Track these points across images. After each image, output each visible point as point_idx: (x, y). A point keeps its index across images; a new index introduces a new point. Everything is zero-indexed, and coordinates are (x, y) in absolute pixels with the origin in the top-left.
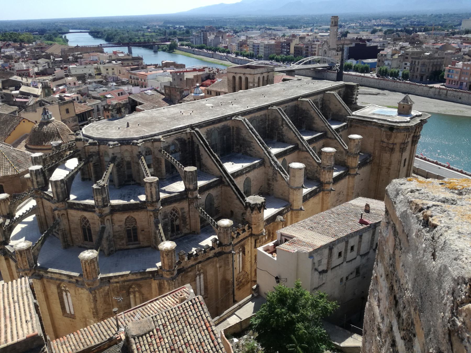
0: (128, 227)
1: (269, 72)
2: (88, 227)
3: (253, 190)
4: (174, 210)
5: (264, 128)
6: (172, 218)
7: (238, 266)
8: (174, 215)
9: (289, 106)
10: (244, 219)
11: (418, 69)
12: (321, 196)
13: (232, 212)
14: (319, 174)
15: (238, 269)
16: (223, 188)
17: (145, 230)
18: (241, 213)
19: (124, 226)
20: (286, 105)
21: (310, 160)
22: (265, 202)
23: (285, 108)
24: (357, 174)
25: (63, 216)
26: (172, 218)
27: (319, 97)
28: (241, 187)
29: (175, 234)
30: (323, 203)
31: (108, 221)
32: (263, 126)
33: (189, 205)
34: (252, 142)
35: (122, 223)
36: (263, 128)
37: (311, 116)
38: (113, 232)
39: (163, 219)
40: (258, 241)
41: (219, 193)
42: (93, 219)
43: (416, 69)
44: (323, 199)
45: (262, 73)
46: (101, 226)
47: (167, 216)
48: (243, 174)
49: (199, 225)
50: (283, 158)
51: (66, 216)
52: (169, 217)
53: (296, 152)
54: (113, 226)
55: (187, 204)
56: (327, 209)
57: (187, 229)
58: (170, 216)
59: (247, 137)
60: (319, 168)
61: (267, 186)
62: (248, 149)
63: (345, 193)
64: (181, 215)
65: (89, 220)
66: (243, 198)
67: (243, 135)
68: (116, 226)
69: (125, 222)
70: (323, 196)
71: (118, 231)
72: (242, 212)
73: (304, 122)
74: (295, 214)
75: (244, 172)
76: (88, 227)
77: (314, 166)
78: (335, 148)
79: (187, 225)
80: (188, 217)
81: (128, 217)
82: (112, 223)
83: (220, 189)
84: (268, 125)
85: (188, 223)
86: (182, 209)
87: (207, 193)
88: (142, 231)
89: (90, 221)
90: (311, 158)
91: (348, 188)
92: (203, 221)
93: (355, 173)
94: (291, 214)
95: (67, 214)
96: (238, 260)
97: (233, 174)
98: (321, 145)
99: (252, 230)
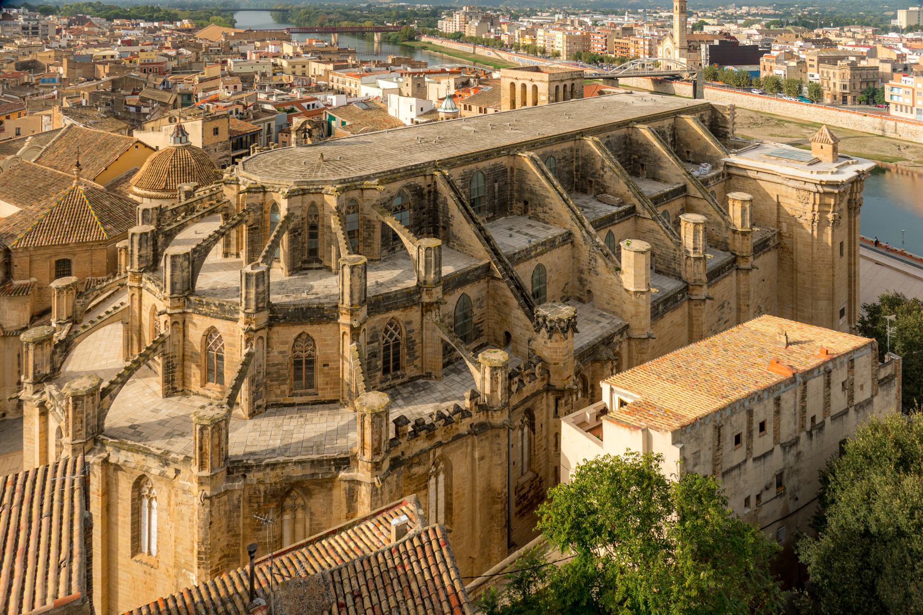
0: (298, 357)
1: (573, 79)
2: (220, 350)
3: (549, 293)
4: (391, 324)
5: (570, 173)
6: (387, 342)
7: (520, 458)
8: (391, 335)
9: (613, 135)
10: (533, 350)
11: (834, 84)
12: (686, 310)
13: (508, 336)
14: (680, 265)
15: (520, 464)
16: (491, 284)
17: (331, 364)
18: (527, 338)
19: (290, 353)
20: (609, 133)
21: (659, 237)
22: (574, 317)
23: (607, 139)
24: (753, 267)
25: (176, 325)
26: (387, 342)
27: (667, 123)
28: (527, 283)
29: (389, 376)
30: (691, 325)
31: (260, 341)
32: (567, 169)
33: (422, 315)
34: (548, 197)
35: (287, 348)
36: (567, 172)
37: (656, 155)
38: (268, 365)
39: (368, 343)
40: (563, 401)
41: (484, 293)
42: (231, 335)
43: (831, 86)
44: (690, 317)
45: (562, 81)
46: (245, 351)
47: (377, 336)
48: (531, 258)
49: (440, 361)
50: (607, 230)
51: (181, 326)
52: (381, 338)
53: (632, 219)
54: (268, 353)
55: (419, 313)
56: (702, 337)
57: (416, 366)
58: (384, 338)
59: (537, 188)
60: (678, 252)
61: (577, 284)
62: (539, 209)
63: (733, 305)
64: (404, 335)
65: (223, 338)
66: (531, 308)
67: (531, 183)
68: (275, 353)
69: (294, 346)
70: (690, 308)
71: (277, 365)
72: (528, 335)
73: (642, 165)
74: (636, 346)
75: (533, 253)
76: (220, 350)
77: (668, 248)
78: (704, 214)
79: (416, 358)
80: (418, 341)
81: (300, 335)
82: (268, 346)
83: (486, 285)
84: (578, 167)
85: (417, 354)
86: (410, 323)
87: (459, 292)
88: (324, 365)
89: (226, 340)
90: (662, 232)
91: (738, 294)
92: (447, 350)
93: (748, 266)
94: (629, 345)
95: (184, 323)
96: (520, 444)
97: (511, 258)
98: (679, 209)
99: (549, 376)
